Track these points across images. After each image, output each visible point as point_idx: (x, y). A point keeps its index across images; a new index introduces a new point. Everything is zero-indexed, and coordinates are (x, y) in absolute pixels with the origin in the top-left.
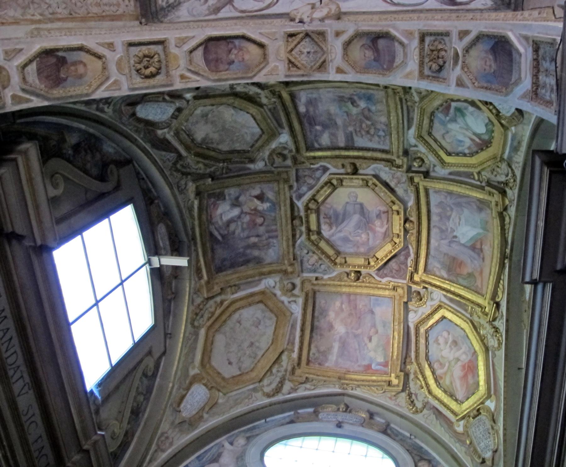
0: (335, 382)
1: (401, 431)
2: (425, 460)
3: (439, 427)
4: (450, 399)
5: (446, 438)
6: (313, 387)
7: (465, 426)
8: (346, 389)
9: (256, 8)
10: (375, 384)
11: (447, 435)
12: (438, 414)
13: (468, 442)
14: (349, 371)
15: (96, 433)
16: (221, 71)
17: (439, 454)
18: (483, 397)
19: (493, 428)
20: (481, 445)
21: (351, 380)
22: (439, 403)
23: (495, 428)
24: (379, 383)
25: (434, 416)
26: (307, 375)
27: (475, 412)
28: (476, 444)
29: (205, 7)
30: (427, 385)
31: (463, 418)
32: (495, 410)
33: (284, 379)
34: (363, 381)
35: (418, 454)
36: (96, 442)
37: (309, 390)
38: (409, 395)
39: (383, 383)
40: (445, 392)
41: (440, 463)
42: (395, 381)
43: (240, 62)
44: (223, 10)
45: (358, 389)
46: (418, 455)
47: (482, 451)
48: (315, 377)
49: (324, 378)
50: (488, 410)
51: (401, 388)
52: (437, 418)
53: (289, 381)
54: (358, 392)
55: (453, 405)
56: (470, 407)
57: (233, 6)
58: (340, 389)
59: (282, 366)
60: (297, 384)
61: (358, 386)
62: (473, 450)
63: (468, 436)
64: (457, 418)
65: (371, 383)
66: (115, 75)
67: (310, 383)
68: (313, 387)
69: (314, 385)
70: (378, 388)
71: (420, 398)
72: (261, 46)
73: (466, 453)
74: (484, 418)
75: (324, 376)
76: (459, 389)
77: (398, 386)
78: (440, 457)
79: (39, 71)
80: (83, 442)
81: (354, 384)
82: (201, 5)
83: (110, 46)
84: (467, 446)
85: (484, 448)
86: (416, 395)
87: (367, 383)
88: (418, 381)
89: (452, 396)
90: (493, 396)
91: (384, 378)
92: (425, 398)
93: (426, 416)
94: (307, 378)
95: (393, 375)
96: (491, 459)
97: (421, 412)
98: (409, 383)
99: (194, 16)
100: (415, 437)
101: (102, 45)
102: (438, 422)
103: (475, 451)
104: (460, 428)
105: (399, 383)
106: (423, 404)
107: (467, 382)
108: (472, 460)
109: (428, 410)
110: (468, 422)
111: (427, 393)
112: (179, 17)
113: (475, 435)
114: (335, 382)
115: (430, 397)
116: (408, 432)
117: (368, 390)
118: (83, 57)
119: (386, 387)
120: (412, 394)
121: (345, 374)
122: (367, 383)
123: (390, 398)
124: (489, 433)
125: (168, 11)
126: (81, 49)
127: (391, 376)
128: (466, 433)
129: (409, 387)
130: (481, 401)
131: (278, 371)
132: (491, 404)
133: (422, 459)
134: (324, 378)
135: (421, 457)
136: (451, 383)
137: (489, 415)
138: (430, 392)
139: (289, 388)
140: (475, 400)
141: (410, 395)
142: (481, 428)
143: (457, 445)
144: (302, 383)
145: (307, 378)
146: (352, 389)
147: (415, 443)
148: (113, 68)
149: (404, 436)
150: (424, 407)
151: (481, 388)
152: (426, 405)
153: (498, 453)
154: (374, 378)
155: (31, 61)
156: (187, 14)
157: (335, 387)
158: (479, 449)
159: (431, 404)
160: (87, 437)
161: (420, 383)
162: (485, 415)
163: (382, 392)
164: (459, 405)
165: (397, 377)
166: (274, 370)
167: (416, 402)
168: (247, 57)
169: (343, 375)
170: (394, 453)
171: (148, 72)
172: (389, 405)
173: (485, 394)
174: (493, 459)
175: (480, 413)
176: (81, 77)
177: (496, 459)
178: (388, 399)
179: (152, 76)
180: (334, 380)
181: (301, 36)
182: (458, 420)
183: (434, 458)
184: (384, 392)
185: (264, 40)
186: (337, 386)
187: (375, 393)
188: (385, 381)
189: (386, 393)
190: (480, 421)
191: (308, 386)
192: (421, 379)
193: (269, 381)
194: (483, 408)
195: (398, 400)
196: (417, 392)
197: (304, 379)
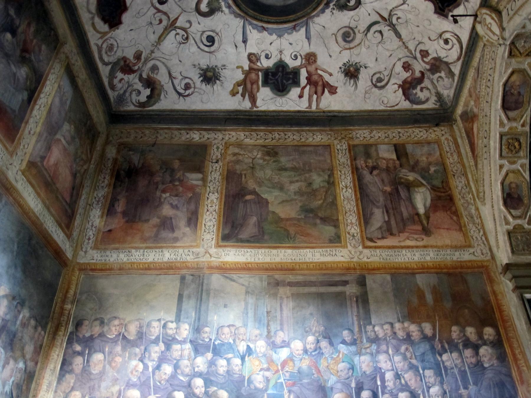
9: (459, 51)
16: (523, 101)
29: (446, 80)
43: (520, 88)
44: (453, 70)
57: (452, 63)
66: (517, 166)
72: (512, 73)
79: (515, 208)
82: (444, 81)
83: (501, 167)
99: (451, 88)
101: (500, 171)
112: (448, 96)
118: (507, 182)
125: (443, 101)
126: (502, 184)
148: (513, 167)
155: (510, 213)
156: (448, 91)
168: (518, 83)
171: (517, 147)
176: (517, 186)
179: (520, 144)
181: (512, 47)
185: (510, 71)
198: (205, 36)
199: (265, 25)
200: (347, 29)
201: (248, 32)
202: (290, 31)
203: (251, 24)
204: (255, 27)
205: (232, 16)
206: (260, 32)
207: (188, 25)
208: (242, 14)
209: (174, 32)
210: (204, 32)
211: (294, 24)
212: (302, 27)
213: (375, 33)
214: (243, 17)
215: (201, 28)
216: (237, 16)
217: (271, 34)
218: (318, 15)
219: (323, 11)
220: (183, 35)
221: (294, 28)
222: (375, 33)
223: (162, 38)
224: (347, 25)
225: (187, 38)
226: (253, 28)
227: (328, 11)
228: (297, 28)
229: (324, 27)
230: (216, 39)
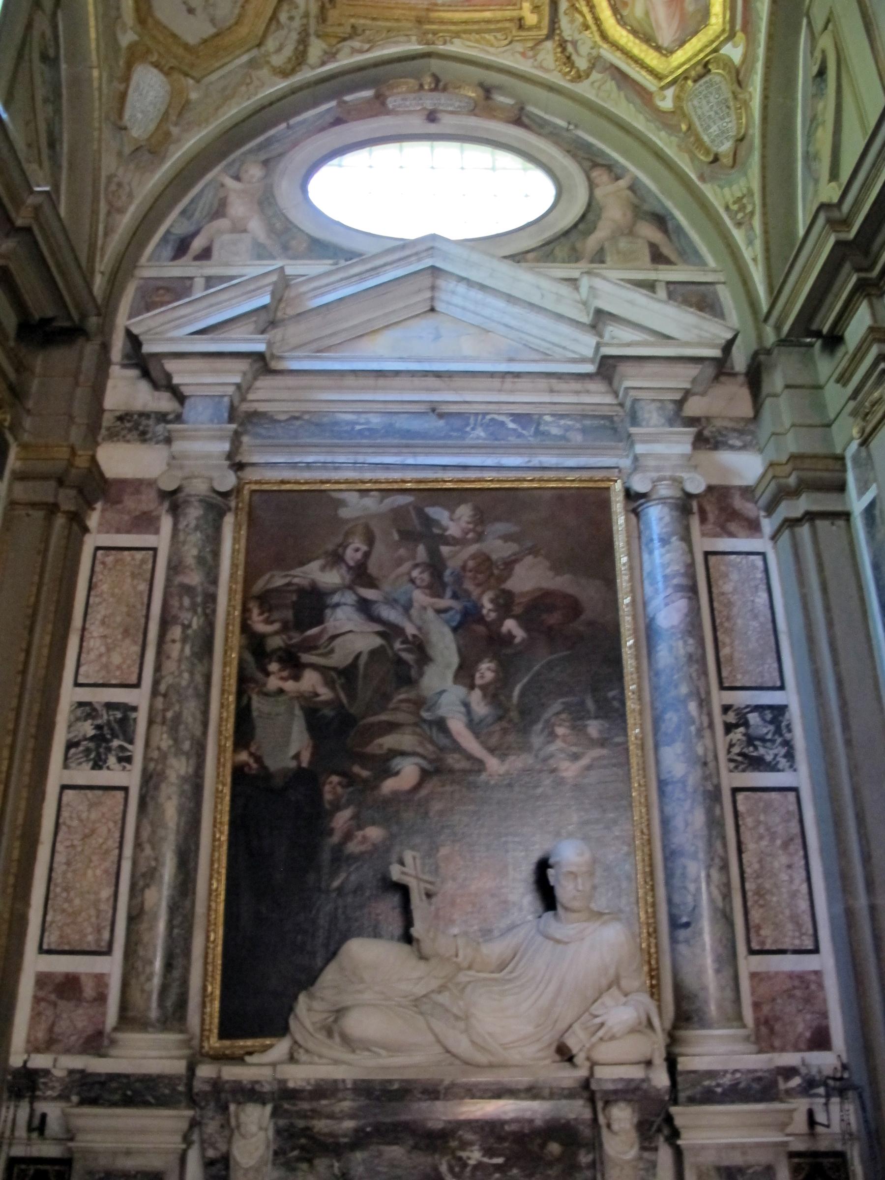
0: (410, 29)
1: (547, 117)
2: (603, 166)
3: (624, 103)
4: (644, 47)
5: (640, 123)
6: (367, 46)
7: (678, 98)
8: (433, 43)
10: (492, 27)
11: (641, 117)
12: (621, 77)
13: (684, 127)
14: (436, 5)
15: (32, 192)
17: (624, 153)
18: (718, 37)
19: (735, 97)
20: (711, 130)
21: (442, 22)
22: (623, 57)
23: (741, 96)
24: (499, 25)
25: (613, 83)
26: (353, 21)
27: (699, 68)
28: (700, 129)
30: (597, 20)
31: (674, 82)
32: (744, 61)
33: (308, 35)
34: (465, 22)
35: (586, 156)
36: (37, 209)
37: (361, 51)
38: (561, 45)
39: (507, 25)
40: (634, 32)
41: (628, 171)
42: (531, 19)
45: (456, 40)
46: (588, 159)
47: (713, 141)
48: (368, 22)
49: (388, 24)
50: (727, 63)
51: (545, 32)
52: (619, 88)
53: (318, 36)
54: (457, 47)
55: (652, 58)
56: (689, 60)
58: (420, 43)
59: (297, 7)
60: (334, 41)
61: (457, 35)
62: (692, 140)
63: (684, 115)
64: (662, 84)
65: (484, 26)
67: (360, 38)
68: (367, 46)
69: (369, 41)
70: (499, 35)
71: (584, 50)
73: (679, 146)
74: (718, 79)
75: (387, 20)
76: (664, 24)
77: (537, 27)
78: (627, 158)
80: (13, 215)
81: (448, 31)
84: (681, 135)
85: (717, 136)
86: (574, 43)
87: (476, 27)
88: (577, 15)
89: (648, 39)
90: (740, 36)
91: (508, 14)
92: (592, 48)
93: (597, 85)
94: (353, 27)
95: (526, 6)
96: (732, 154)
97: (588, 76)
98: (559, 22)
100: (576, 126)
102: (622, 94)
103: (699, 142)
104: (666, 103)
105: (540, 21)
106: (590, 61)
107: (682, 9)
108: (693, 158)
109: (600, 72)
110: (682, 88)
111: (598, 38)
113: (699, 112)
114: (410, 29)
115: (605, 46)
116: (561, 117)
117: (477, 41)
119: (514, 33)
120: (566, 41)
121: (428, 10)
122: (476, 27)
123: (523, 54)
124: (728, 107)
127: (521, 8)
128: (679, 111)
129: (559, 28)
130: (714, 45)
131: (291, 18)
132: (734, 52)
133: (595, 165)
134: (388, 24)
135: (592, 161)
136: (647, 14)
137: (729, 72)
138: (604, 36)
139: (320, 53)
140: (699, 46)
141: (563, 44)
142: (712, 99)
143: (663, 134)
144: (344, 39)
145: (353, 27)
146: (445, 43)
147: (578, 137)
149: (556, 126)
150: (592, 67)
151: (713, 20)
152: (596, 62)
153: (745, 143)
154: (487, 15)
157: (409, 41)
158: (706, 138)
159: (605, 60)
160: (18, 203)
161: (581, 19)
162: (719, 74)
163: (506, 42)
164: (664, 59)
165: (536, 8)
166: (283, 17)
167: (574, 57)
169: (423, 13)
170: (544, 160)
172: (522, 68)
173: (723, 31)
174: (735, 154)
175: (709, 71)
177: (742, 153)
178: (518, 56)
180: (409, 25)
182: (662, 88)
183: (617, 162)
184: (511, 42)
186: (414, 38)
187: (492, 46)
188: (511, 20)
189: (515, 44)
190: (711, 84)
191: (356, 44)
192: (585, 10)
193: (277, 44)
194: (717, 60)
195: (540, 57)
196: (577, 36)
197: (348, 29)
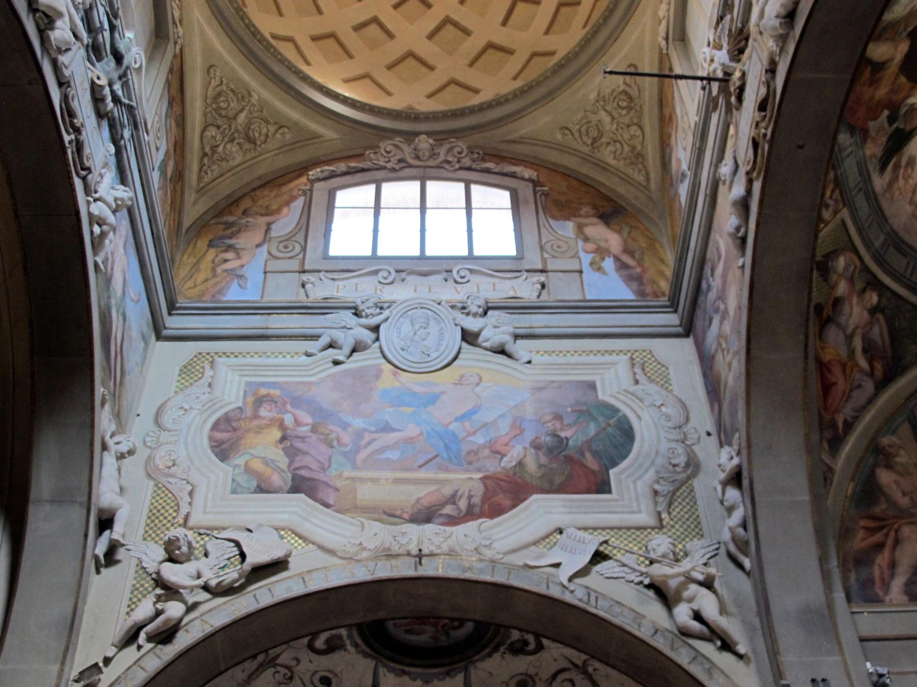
198: (318, 676)
199: (406, 669)
200: (524, 677)
201: (381, 675)
202: (441, 677)
203: (385, 666)
204: (391, 670)
205: (360, 656)
206: (397, 675)
207: (294, 663)
208: (374, 654)
209: (272, 670)
210: (317, 672)
211: (448, 668)
212: (460, 672)
213: (563, 681)
214: (375, 658)
215: (312, 667)
216: (366, 655)
217: (414, 680)
218: (482, 660)
219: (490, 655)
220: (285, 674)
221: (448, 674)
222: (563, 681)
223: (254, 676)
224: (524, 672)
225: (291, 678)
226: (389, 671)
227: (497, 656)
228: (452, 674)
229: (491, 673)
230: (334, 681)
